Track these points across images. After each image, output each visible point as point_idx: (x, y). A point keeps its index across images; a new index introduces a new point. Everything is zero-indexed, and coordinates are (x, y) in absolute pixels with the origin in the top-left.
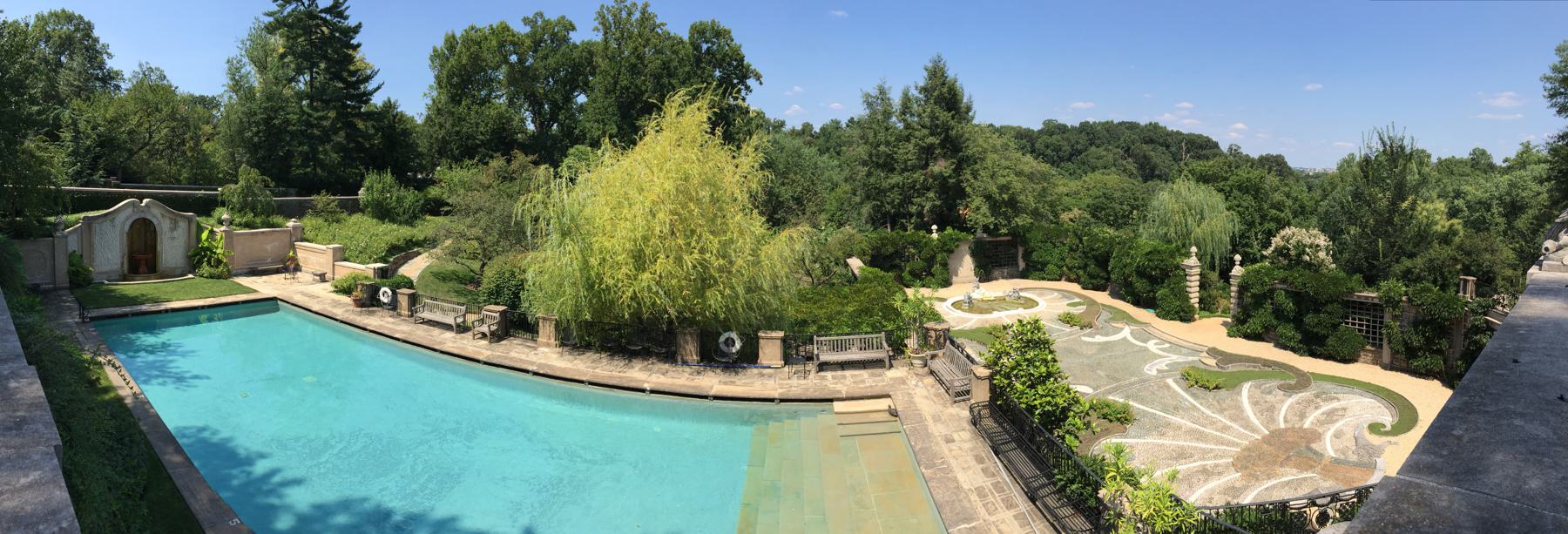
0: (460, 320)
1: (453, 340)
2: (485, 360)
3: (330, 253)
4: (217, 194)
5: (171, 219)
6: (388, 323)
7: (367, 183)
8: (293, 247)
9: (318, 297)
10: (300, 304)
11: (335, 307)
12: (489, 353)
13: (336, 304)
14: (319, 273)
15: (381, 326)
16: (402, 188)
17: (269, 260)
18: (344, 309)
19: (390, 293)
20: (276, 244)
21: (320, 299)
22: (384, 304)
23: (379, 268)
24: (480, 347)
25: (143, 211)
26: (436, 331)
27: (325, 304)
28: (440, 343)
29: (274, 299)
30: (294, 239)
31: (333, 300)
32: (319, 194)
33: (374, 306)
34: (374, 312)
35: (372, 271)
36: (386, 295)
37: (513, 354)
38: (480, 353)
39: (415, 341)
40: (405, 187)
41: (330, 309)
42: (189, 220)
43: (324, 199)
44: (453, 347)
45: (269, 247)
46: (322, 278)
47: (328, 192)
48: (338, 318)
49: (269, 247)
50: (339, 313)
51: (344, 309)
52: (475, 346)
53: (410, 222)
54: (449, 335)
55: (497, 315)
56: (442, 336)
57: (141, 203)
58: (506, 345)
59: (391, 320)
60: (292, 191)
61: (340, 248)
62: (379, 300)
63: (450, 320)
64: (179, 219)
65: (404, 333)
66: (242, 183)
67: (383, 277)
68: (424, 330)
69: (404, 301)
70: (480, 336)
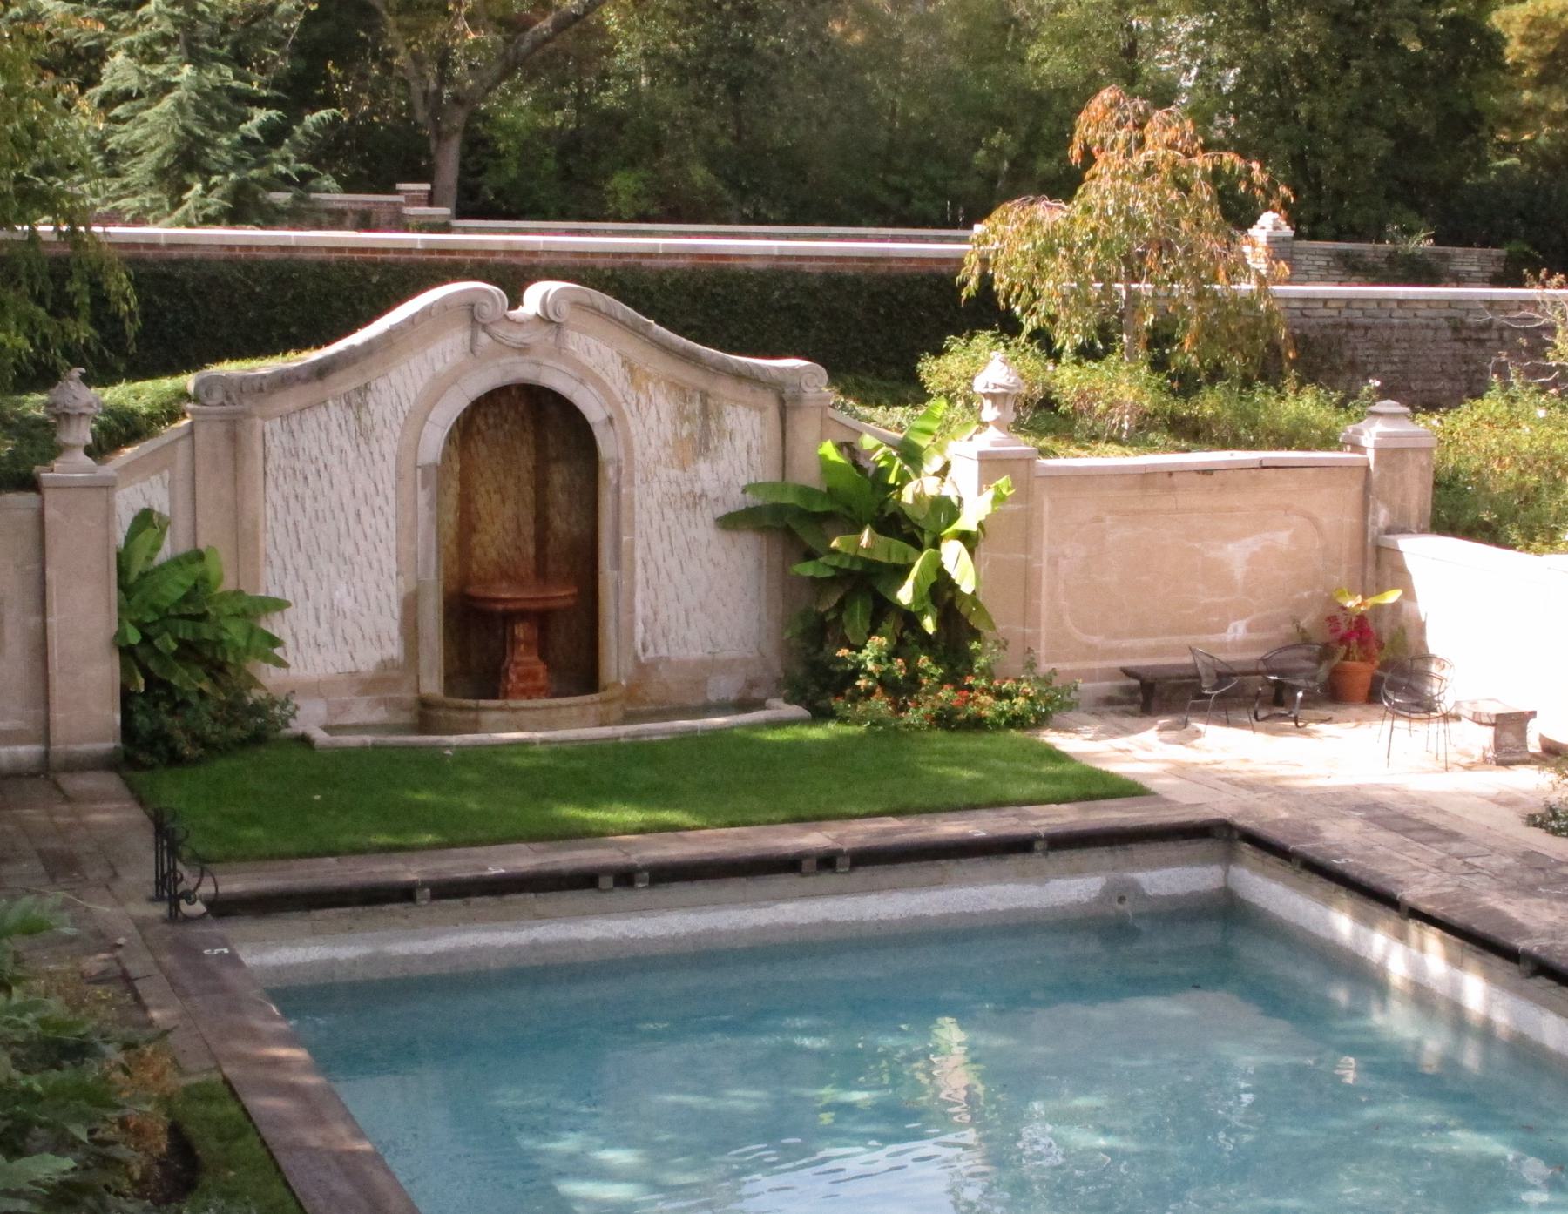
4: (959, 262)
5: (681, 391)
9: (1454, 836)
20: (1283, 538)
21: (1456, 847)
30: (1382, 516)
45: (1237, 555)
49: (1237, 555)
60: (1467, 258)
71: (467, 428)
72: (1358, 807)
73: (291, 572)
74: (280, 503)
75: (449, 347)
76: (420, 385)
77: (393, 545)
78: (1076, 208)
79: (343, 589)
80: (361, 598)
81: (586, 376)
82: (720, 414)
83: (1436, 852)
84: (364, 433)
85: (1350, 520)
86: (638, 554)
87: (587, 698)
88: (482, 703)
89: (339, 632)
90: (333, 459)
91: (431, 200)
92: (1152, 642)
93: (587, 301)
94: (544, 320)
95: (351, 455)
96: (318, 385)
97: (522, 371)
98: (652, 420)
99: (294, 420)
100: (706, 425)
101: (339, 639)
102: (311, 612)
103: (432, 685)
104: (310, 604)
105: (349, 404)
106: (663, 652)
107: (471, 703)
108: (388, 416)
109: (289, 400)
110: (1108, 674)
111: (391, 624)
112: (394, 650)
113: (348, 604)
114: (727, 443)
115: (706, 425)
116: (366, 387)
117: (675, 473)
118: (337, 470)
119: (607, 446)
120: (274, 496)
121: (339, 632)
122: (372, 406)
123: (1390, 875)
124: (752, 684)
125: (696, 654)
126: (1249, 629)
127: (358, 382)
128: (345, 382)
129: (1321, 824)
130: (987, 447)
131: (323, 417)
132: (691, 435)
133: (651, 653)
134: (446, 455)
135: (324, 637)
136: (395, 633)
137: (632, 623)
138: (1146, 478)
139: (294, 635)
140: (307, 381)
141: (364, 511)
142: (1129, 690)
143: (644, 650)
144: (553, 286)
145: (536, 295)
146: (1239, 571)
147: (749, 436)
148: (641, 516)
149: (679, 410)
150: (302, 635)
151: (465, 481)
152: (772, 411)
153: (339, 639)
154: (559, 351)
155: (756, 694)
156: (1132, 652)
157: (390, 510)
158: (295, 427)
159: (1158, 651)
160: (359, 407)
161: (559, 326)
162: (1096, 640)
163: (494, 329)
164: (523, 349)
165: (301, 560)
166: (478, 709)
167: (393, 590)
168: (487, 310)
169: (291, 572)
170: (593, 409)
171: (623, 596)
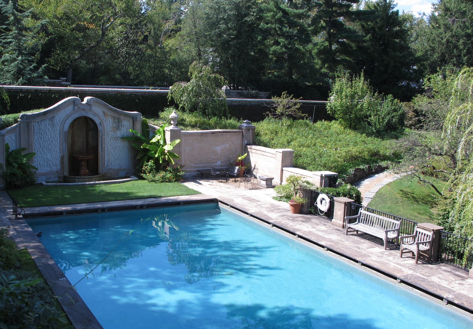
0: (392, 235)
1: (380, 255)
2: (402, 278)
3: (280, 156)
4: (167, 93)
6: (318, 230)
7: (336, 86)
8: (245, 150)
9: (258, 201)
10: (237, 207)
11: (272, 211)
12: (410, 272)
13: (274, 209)
14: (267, 177)
15: (310, 232)
16: (376, 94)
17: (219, 162)
18: (280, 214)
19: (328, 200)
20: (227, 145)
21: (259, 203)
22: (322, 212)
23: (327, 176)
24: (403, 266)
25: (84, 110)
26: (365, 244)
27: (262, 207)
28: (365, 255)
29: (215, 201)
30: (246, 142)
31: (272, 205)
32: (279, 96)
33: (310, 213)
34: (310, 219)
35: (320, 177)
36: (323, 202)
37: (435, 279)
38: (401, 271)
39: (338, 251)
40: (380, 93)
41: (265, 213)
42: (134, 119)
43: (285, 101)
44: (376, 261)
45: (219, 149)
46: (269, 183)
47: (289, 93)
48: (270, 221)
49: (219, 149)
50: (274, 217)
51: (280, 214)
52: (398, 264)
53: (380, 134)
54: (378, 249)
55: (430, 234)
56: (371, 250)
57: (83, 100)
58: (432, 268)
59: (324, 228)
61: (291, 153)
62: (316, 208)
63: (381, 234)
64: (122, 117)
65: (332, 241)
66: (193, 80)
67: (330, 186)
68: (354, 242)
69: (339, 211)
70: (410, 255)
71: (73, 124)
72: (241, 196)
73: (39, 152)
74: (37, 139)
75: (70, 109)
76: (64, 116)
77: (59, 147)
78: (189, 84)
79: (49, 155)
80: (53, 157)
81: (96, 115)
82: (121, 122)
83: (255, 204)
84: (53, 125)
85: (240, 142)
86: (106, 148)
87: (96, 176)
88: (76, 177)
89: (48, 163)
90: (47, 130)
91: (67, 81)
92: (203, 165)
93: (96, 100)
94: (88, 103)
95: (51, 129)
96: (44, 116)
97: (84, 114)
98: (108, 124)
99: (40, 123)
100: (119, 124)
101: (48, 165)
102: (43, 160)
103: (66, 174)
104: (43, 158)
105: (50, 120)
106: (111, 167)
107: (74, 177)
108: (58, 122)
109: (38, 119)
110: (195, 171)
111: (58, 162)
112: (59, 167)
113: (50, 158)
114: (123, 128)
115: (119, 124)
116: (54, 117)
117: (113, 133)
118: (48, 132)
119: (100, 128)
120: (36, 137)
121: (48, 163)
122: (55, 120)
123: (247, 208)
124: (127, 173)
125: (117, 167)
126: (221, 163)
127: (52, 116)
128: (50, 116)
129: (234, 199)
130: (172, 128)
131: (45, 122)
132: (116, 126)
133: (108, 167)
134: (69, 130)
135: (45, 164)
136: (59, 164)
137: (105, 161)
138: (202, 134)
139: (40, 164)
140: (42, 115)
141: (53, 140)
142: (198, 174)
143: (107, 167)
144: (90, 97)
145: (86, 99)
146: (219, 152)
147: (127, 126)
148: (106, 141)
149: (114, 121)
150: (41, 164)
151: (72, 134)
152: (131, 121)
153: (48, 165)
154: (90, 109)
155: (128, 175)
156: (199, 167)
157: (58, 140)
158: (40, 124)
159: (204, 167)
160: (52, 120)
161: (91, 105)
162: (192, 165)
163: (78, 106)
164: (84, 110)
165: (41, 150)
166: (75, 178)
167: (59, 156)
168: (77, 102)
169: (39, 152)
170: (97, 122)
171: (103, 156)
